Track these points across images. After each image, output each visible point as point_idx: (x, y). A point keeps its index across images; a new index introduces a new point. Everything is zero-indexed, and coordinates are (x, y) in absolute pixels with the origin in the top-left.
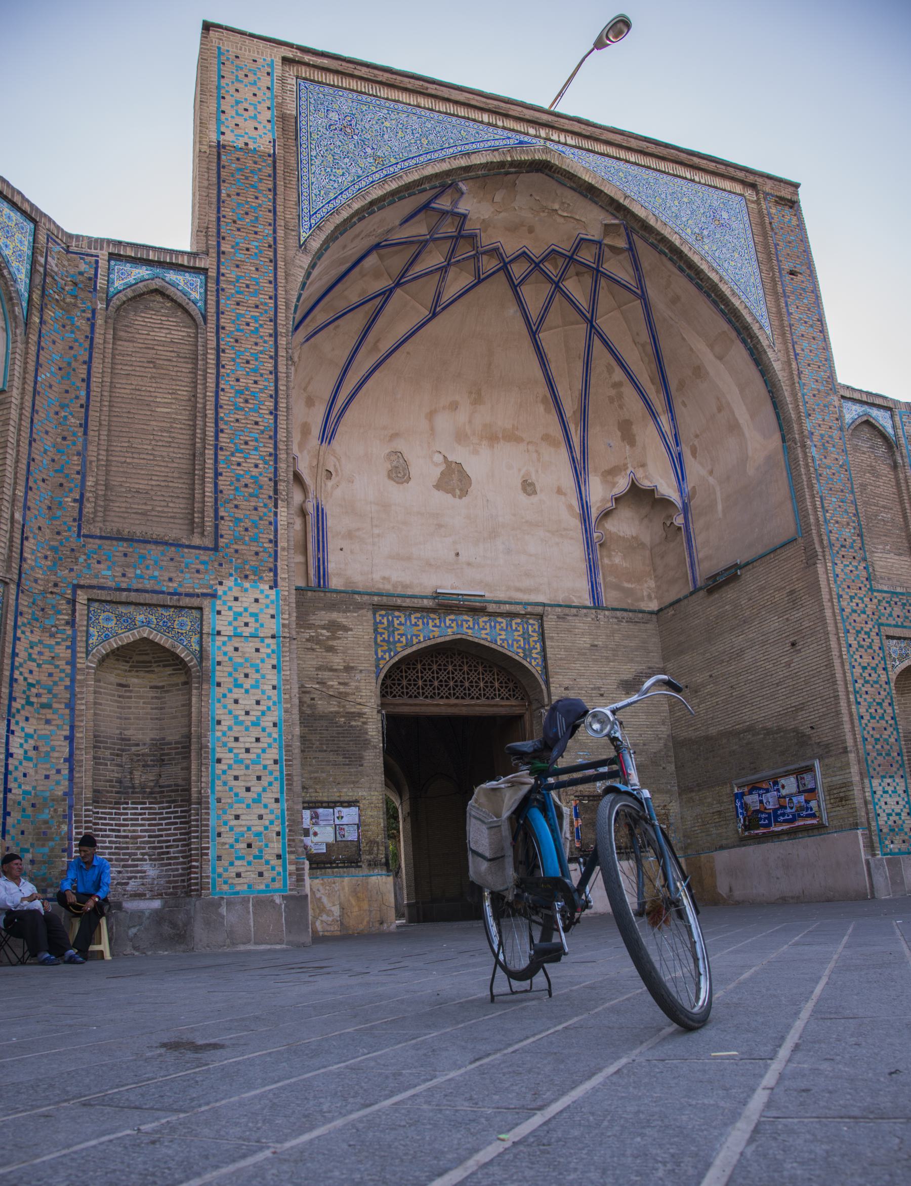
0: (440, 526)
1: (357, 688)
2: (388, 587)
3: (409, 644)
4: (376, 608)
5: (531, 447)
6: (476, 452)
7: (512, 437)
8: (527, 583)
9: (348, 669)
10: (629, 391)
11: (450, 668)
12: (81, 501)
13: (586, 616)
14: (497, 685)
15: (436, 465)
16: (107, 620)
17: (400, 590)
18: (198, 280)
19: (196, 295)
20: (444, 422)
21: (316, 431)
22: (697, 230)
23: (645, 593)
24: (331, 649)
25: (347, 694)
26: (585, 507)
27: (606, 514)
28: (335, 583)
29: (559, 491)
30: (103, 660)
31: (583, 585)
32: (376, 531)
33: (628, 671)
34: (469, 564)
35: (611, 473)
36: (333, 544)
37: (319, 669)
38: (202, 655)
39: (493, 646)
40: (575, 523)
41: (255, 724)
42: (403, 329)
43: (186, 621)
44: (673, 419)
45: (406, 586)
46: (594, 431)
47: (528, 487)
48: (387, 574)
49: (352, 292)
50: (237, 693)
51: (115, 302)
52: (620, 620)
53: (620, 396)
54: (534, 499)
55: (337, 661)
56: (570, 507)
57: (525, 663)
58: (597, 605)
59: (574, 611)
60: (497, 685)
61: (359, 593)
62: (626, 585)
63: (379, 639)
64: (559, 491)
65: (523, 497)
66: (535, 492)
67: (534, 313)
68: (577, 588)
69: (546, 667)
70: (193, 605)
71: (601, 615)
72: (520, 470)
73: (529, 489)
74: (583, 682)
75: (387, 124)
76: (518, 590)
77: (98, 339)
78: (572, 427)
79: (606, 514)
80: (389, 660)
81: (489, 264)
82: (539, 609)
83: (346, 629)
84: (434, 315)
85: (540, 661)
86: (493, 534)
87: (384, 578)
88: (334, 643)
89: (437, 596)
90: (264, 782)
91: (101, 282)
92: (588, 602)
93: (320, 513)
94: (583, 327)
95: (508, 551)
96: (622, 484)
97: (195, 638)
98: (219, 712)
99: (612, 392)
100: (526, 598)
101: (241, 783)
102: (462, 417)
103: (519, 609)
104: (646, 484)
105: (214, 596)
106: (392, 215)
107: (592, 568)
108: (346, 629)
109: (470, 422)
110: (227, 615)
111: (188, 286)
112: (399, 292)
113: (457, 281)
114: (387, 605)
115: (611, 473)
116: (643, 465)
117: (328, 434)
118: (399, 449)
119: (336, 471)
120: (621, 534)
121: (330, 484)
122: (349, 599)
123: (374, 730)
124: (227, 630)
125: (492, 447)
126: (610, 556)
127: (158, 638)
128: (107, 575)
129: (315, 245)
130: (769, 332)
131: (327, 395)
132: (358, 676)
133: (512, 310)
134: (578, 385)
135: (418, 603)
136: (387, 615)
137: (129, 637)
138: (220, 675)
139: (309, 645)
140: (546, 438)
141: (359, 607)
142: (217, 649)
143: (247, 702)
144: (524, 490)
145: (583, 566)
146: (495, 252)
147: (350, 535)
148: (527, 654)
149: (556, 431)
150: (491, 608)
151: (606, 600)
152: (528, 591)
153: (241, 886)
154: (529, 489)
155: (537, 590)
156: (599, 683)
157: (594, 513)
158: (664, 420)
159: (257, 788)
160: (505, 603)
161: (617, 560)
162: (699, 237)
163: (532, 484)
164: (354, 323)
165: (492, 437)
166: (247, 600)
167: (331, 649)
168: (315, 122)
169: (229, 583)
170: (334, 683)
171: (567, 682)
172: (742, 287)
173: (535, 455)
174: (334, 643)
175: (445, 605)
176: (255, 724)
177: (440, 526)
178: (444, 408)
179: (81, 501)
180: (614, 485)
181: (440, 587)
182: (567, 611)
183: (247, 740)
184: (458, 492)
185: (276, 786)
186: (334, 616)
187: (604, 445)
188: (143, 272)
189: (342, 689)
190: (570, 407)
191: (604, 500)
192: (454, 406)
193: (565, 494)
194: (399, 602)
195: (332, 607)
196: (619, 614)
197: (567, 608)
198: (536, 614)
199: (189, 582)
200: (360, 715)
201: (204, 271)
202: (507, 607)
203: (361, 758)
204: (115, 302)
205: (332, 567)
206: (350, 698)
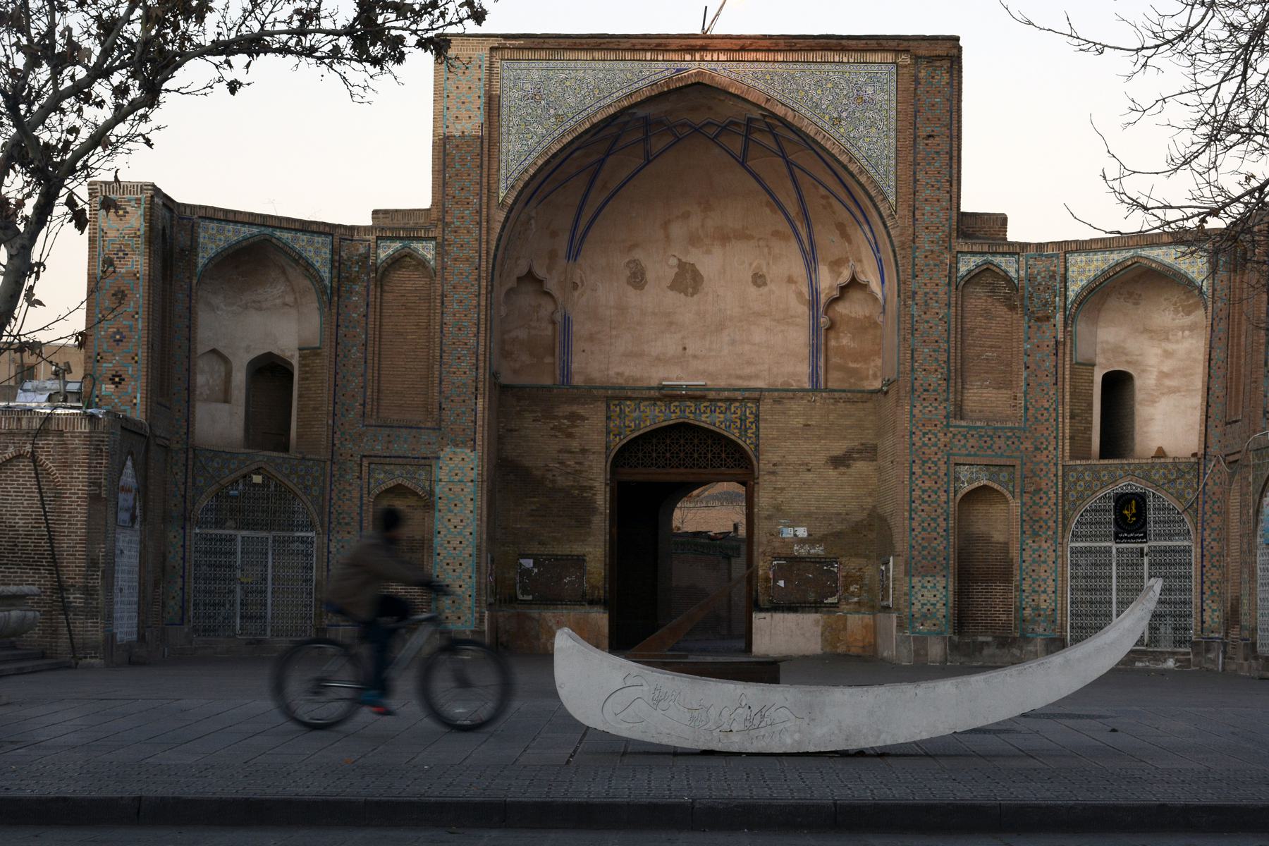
0: (671, 323)
1: (590, 467)
2: (621, 381)
3: (638, 427)
4: (608, 400)
5: (761, 243)
6: (708, 252)
7: (743, 236)
8: (748, 370)
9: (584, 451)
10: (833, 200)
11: (682, 441)
12: (364, 405)
13: (802, 398)
14: (723, 455)
15: (672, 267)
17: (631, 384)
18: (431, 245)
19: (429, 257)
20: (677, 230)
21: (562, 252)
22: (835, 115)
23: (871, 372)
24: (570, 435)
25: (581, 472)
26: (815, 293)
27: (833, 301)
28: (577, 380)
29: (790, 280)
31: (804, 369)
32: (614, 333)
33: (839, 448)
34: (695, 357)
35: (836, 264)
36: (577, 346)
37: (560, 451)
39: (712, 428)
40: (802, 310)
41: (460, 534)
42: (625, 174)
43: (422, 474)
44: (872, 231)
45: (636, 380)
46: (817, 229)
47: (759, 280)
48: (620, 370)
51: (380, 271)
52: (836, 401)
53: (830, 205)
54: (764, 290)
55: (575, 445)
56: (800, 294)
57: (740, 441)
58: (815, 389)
59: (791, 394)
60: (723, 455)
61: (595, 388)
62: (851, 365)
63: (612, 425)
64: (790, 280)
65: (752, 290)
66: (765, 284)
68: (798, 372)
69: (757, 446)
70: (427, 462)
72: (751, 265)
73: (759, 281)
74: (792, 458)
75: (568, 83)
76: (739, 377)
77: (372, 299)
78: (798, 224)
80: (617, 443)
82: (756, 394)
83: (583, 418)
84: (649, 162)
85: (753, 440)
86: (721, 327)
87: (618, 374)
88: (573, 430)
89: (662, 388)
90: (464, 567)
92: (807, 386)
93: (567, 320)
95: (733, 343)
96: (845, 277)
97: (427, 483)
98: (438, 526)
99: (824, 202)
100: (745, 384)
101: (450, 567)
102: (695, 222)
103: (738, 395)
104: (862, 278)
105: (438, 458)
107: (815, 351)
108: (583, 418)
109: (703, 226)
110: (446, 470)
113: (657, 144)
114: (617, 396)
115: (836, 264)
116: (860, 261)
117: (574, 253)
118: (637, 257)
119: (582, 282)
120: (853, 315)
121: (576, 294)
123: (602, 500)
124: (445, 478)
125: (724, 246)
126: (837, 338)
127: (407, 483)
129: (510, 201)
130: (892, 199)
132: (591, 457)
134: (794, 195)
135: (646, 394)
136: (619, 405)
137: (391, 484)
138: (440, 505)
139: (553, 432)
140: (776, 234)
143: (455, 521)
145: (806, 351)
146: (684, 125)
147: (591, 338)
149: (784, 227)
150: (712, 395)
151: (826, 381)
152: (749, 377)
154: (759, 281)
155: (757, 377)
156: (808, 459)
157: (823, 299)
158: (866, 228)
159: (459, 570)
160: (724, 390)
161: (845, 341)
162: (837, 121)
163: (762, 276)
165: (724, 238)
166: (457, 460)
167: (570, 435)
168: (510, 98)
170: (571, 463)
171: (776, 459)
172: (873, 162)
173: (766, 250)
174: (573, 430)
175: (667, 395)
176: (460, 534)
177: (671, 323)
178: (678, 217)
179: (364, 405)
180: (840, 274)
181: (665, 379)
182: (783, 394)
183: (455, 543)
184: (690, 290)
185: (470, 570)
186: (575, 408)
187: (827, 239)
188: (398, 245)
189: (578, 467)
190: (793, 209)
191: (831, 287)
192: (686, 216)
193: (795, 283)
196: (837, 395)
197: (783, 395)
198: (751, 399)
199: (424, 451)
200: (591, 488)
201: (434, 238)
203: (590, 522)
204: (380, 271)
205: (575, 366)
206: (584, 474)
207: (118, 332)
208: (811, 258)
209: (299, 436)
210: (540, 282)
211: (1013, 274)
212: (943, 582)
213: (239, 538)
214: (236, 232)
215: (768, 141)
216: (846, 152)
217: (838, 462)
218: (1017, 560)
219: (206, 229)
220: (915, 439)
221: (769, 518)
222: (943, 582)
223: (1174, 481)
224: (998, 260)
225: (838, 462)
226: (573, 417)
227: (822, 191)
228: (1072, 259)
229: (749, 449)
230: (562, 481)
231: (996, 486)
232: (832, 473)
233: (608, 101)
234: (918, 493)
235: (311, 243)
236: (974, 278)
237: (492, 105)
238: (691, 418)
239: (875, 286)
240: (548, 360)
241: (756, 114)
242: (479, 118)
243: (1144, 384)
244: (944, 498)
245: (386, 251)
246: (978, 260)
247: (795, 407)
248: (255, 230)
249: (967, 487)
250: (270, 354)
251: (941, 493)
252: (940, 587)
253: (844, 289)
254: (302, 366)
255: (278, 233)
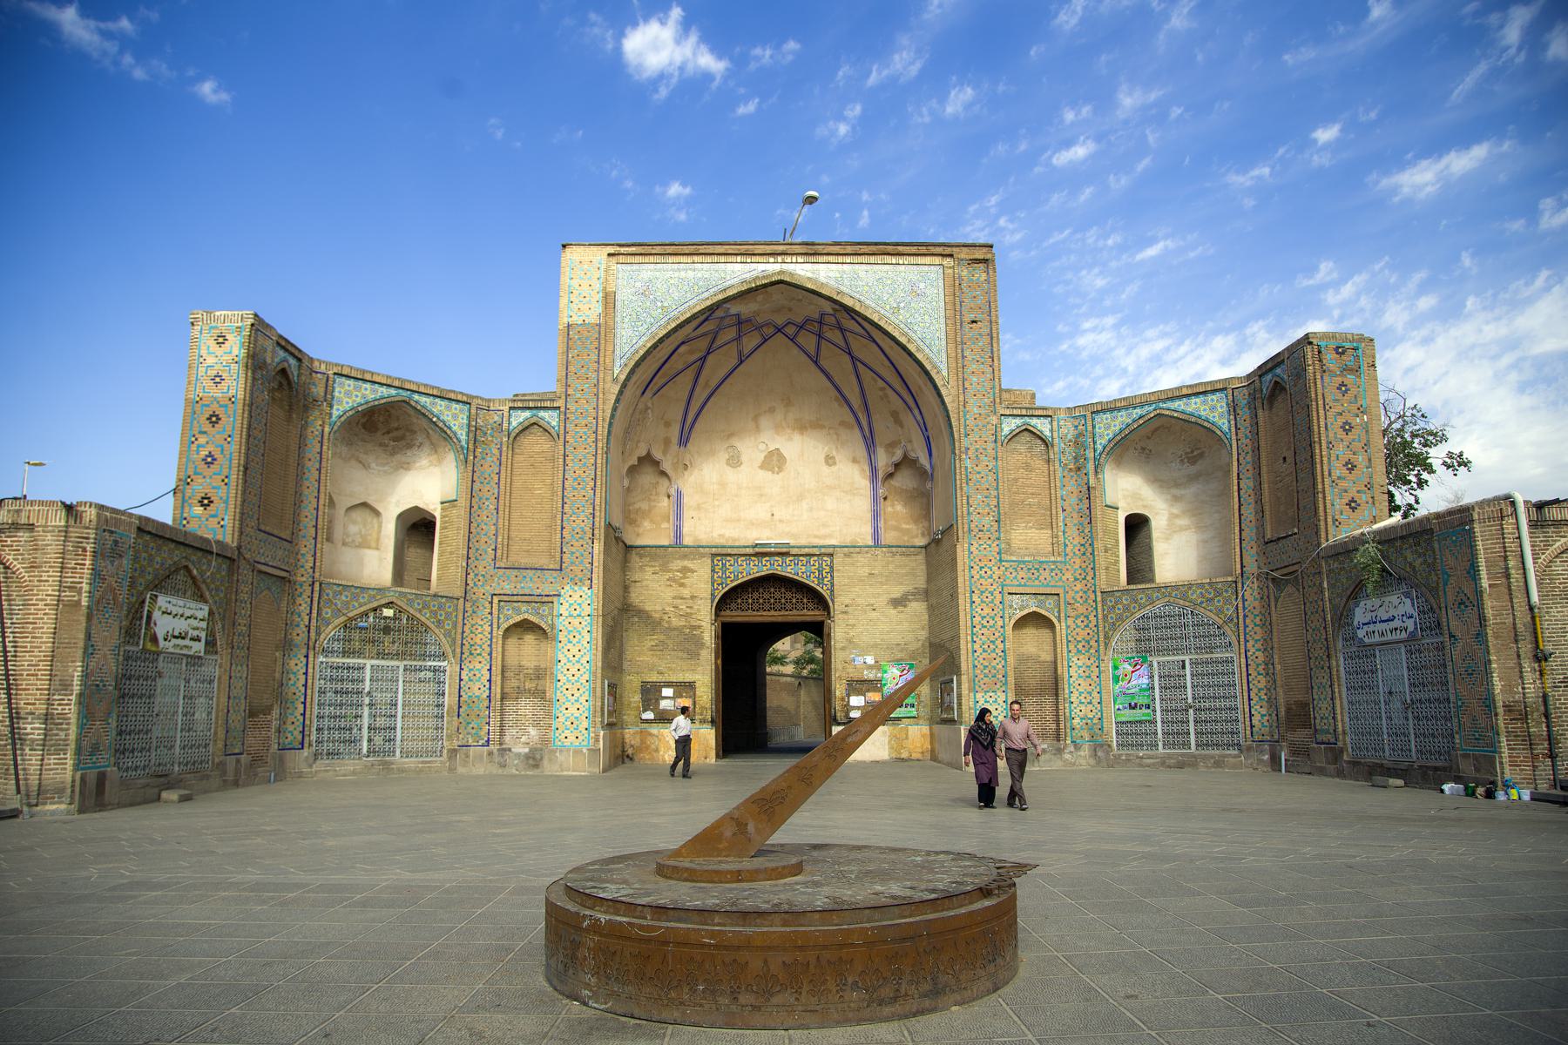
2: (722, 542)
4: (714, 555)
6: (790, 439)
8: (823, 531)
9: (693, 597)
10: (890, 392)
16: (508, 610)
18: (555, 413)
21: (675, 440)
28: (687, 541)
30: (507, 630)
33: (897, 592)
36: (687, 514)
38: (553, 627)
42: (722, 373)
46: (874, 418)
49: (677, 363)
50: (570, 646)
52: (894, 554)
53: (886, 396)
54: (834, 468)
55: (686, 592)
58: (877, 544)
65: (825, 469)
67: (812, 352)
68: (864, 534)
70: (547, 600)
71: (878, 551)
74: (859, 601)
77: (504, 459)
79: (890, 476)
81: (769, 331)
82: (830, 550)
86: (801, 498)
91: (505, 425)
92: (871, 543)
94: (847, 358)
95: (811, 509)
96: (898, 455)
104: (913, 455)
106: (688, 329)
107: (876, 516)
111: (551, 418)
112: (710, 358)
113: (750, 342)
114: (720, 555)
115: (891, 446)
117: (684, 441)
122: (697, 550)
123: (709, 635)
124: (566, 614)
128: (508, 588)
129: (623, 377)
130: (945, 373)
131: (680, 418)
133: (796, 350)
134: (857, 390)
137: (518, 619)
138: (561, 636)
141: (702, 556)
142: (561, 623)
144: (827, 463)
145: (869, 516)
146: (768, 325)
147: (698, 508)
148: (821, 579)
149: (852, 420)
150: (794, 551)
152: (825, 537)
153: (567, 743)
155: (830, 536)
158: (916, 412)
159: (577, 694)
164: (686, 379)
167: (682, 585)
168: (624, 295)
169: (567, 588)
171: (847, 601)
175: (761, 553)
183: (574, 670)
186: (686, 563)
187: (882, 425)
188: (527, 414)
190: (856, 402)
194: (729, 551)
195: (685, 557)
197: (852, 549)
199: (547, 589)
202: (806, 551)
205: (685, 530)
207: (210, 455)
208: (870, 443)
209: (439, 578)
210: (657, 463)
211: (1048, 433)
212: (1002, 697)
213: (368, 667)
214: (373, 391)
215: (836, 336)
216: (905, 334)
217: (897, 603)
218: (1066, 676)
219: (342, 385)
220: (974, 572)
221: (843, 649)
222: (1002, 697)
223: (1212, 599)
224: (1034, 421)
225: (897, 603)
226: (685, 570)
227: (881, 383)
228: (1097, 418)
229: (826, 594)
230: (676, 622)
231: (1043, 612)
232: (893, 612)
233: (706, 295)
234: (977, 620)
235: (448, 408)
236: (1014, 436)
237: (609, 300)
238: (780, 571)
239: (924, 461)
240: (665, 525)
241: (828, 308)
242: (599, 309)
243: (1158, 525)
244: (1000, 623)
245: (520, 417)
246: (1019, 421)
247: (861, 559)
248: (393, 392)
249: (1020, 614)
250: (416, 509)
251: (998, 619)
252: (1000, 701)
253: (897, 466)
254: (443, 517)
255: (416, 397)
